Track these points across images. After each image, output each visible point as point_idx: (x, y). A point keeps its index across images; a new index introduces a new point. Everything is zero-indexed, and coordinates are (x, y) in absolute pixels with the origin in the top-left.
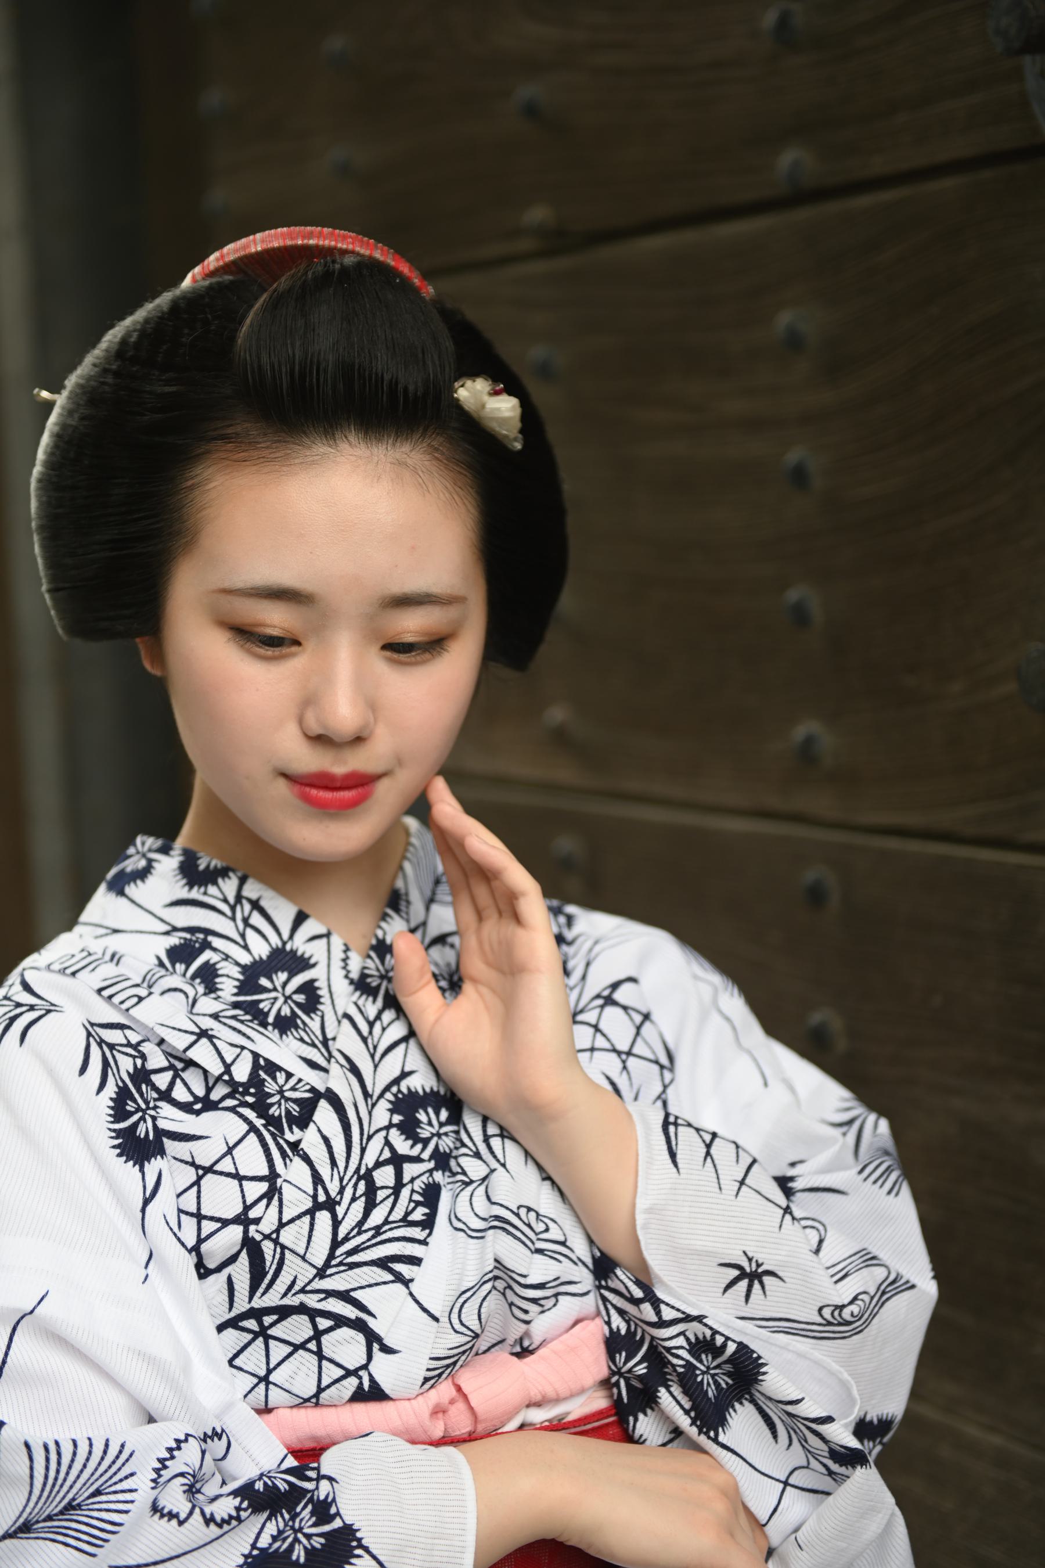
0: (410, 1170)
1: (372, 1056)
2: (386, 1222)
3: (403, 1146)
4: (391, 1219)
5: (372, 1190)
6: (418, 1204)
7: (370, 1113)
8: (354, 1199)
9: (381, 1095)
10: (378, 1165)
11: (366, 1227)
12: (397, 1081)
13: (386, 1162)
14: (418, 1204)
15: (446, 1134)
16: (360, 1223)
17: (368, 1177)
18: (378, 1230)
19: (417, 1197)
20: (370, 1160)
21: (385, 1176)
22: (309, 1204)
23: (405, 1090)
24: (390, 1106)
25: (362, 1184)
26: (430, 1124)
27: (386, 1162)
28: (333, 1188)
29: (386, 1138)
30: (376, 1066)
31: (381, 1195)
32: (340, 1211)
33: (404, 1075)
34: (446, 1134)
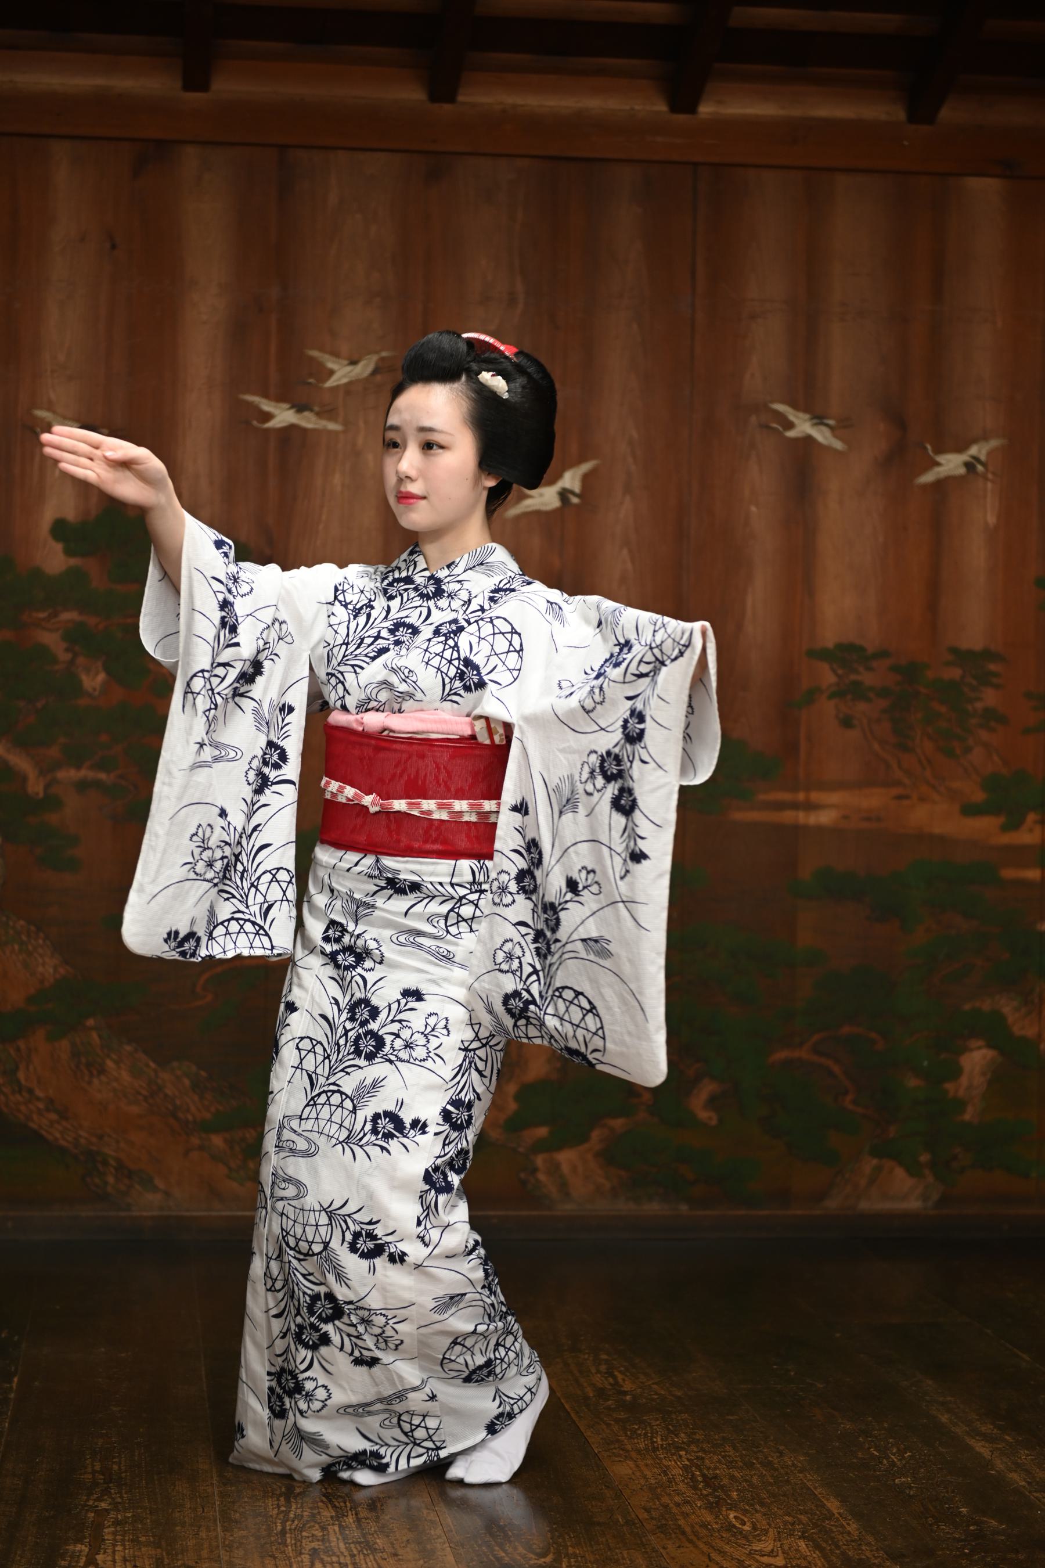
2: (343, 1056)
8: (334, 1052)
22: (322, 1058)
32: (331, 1058)
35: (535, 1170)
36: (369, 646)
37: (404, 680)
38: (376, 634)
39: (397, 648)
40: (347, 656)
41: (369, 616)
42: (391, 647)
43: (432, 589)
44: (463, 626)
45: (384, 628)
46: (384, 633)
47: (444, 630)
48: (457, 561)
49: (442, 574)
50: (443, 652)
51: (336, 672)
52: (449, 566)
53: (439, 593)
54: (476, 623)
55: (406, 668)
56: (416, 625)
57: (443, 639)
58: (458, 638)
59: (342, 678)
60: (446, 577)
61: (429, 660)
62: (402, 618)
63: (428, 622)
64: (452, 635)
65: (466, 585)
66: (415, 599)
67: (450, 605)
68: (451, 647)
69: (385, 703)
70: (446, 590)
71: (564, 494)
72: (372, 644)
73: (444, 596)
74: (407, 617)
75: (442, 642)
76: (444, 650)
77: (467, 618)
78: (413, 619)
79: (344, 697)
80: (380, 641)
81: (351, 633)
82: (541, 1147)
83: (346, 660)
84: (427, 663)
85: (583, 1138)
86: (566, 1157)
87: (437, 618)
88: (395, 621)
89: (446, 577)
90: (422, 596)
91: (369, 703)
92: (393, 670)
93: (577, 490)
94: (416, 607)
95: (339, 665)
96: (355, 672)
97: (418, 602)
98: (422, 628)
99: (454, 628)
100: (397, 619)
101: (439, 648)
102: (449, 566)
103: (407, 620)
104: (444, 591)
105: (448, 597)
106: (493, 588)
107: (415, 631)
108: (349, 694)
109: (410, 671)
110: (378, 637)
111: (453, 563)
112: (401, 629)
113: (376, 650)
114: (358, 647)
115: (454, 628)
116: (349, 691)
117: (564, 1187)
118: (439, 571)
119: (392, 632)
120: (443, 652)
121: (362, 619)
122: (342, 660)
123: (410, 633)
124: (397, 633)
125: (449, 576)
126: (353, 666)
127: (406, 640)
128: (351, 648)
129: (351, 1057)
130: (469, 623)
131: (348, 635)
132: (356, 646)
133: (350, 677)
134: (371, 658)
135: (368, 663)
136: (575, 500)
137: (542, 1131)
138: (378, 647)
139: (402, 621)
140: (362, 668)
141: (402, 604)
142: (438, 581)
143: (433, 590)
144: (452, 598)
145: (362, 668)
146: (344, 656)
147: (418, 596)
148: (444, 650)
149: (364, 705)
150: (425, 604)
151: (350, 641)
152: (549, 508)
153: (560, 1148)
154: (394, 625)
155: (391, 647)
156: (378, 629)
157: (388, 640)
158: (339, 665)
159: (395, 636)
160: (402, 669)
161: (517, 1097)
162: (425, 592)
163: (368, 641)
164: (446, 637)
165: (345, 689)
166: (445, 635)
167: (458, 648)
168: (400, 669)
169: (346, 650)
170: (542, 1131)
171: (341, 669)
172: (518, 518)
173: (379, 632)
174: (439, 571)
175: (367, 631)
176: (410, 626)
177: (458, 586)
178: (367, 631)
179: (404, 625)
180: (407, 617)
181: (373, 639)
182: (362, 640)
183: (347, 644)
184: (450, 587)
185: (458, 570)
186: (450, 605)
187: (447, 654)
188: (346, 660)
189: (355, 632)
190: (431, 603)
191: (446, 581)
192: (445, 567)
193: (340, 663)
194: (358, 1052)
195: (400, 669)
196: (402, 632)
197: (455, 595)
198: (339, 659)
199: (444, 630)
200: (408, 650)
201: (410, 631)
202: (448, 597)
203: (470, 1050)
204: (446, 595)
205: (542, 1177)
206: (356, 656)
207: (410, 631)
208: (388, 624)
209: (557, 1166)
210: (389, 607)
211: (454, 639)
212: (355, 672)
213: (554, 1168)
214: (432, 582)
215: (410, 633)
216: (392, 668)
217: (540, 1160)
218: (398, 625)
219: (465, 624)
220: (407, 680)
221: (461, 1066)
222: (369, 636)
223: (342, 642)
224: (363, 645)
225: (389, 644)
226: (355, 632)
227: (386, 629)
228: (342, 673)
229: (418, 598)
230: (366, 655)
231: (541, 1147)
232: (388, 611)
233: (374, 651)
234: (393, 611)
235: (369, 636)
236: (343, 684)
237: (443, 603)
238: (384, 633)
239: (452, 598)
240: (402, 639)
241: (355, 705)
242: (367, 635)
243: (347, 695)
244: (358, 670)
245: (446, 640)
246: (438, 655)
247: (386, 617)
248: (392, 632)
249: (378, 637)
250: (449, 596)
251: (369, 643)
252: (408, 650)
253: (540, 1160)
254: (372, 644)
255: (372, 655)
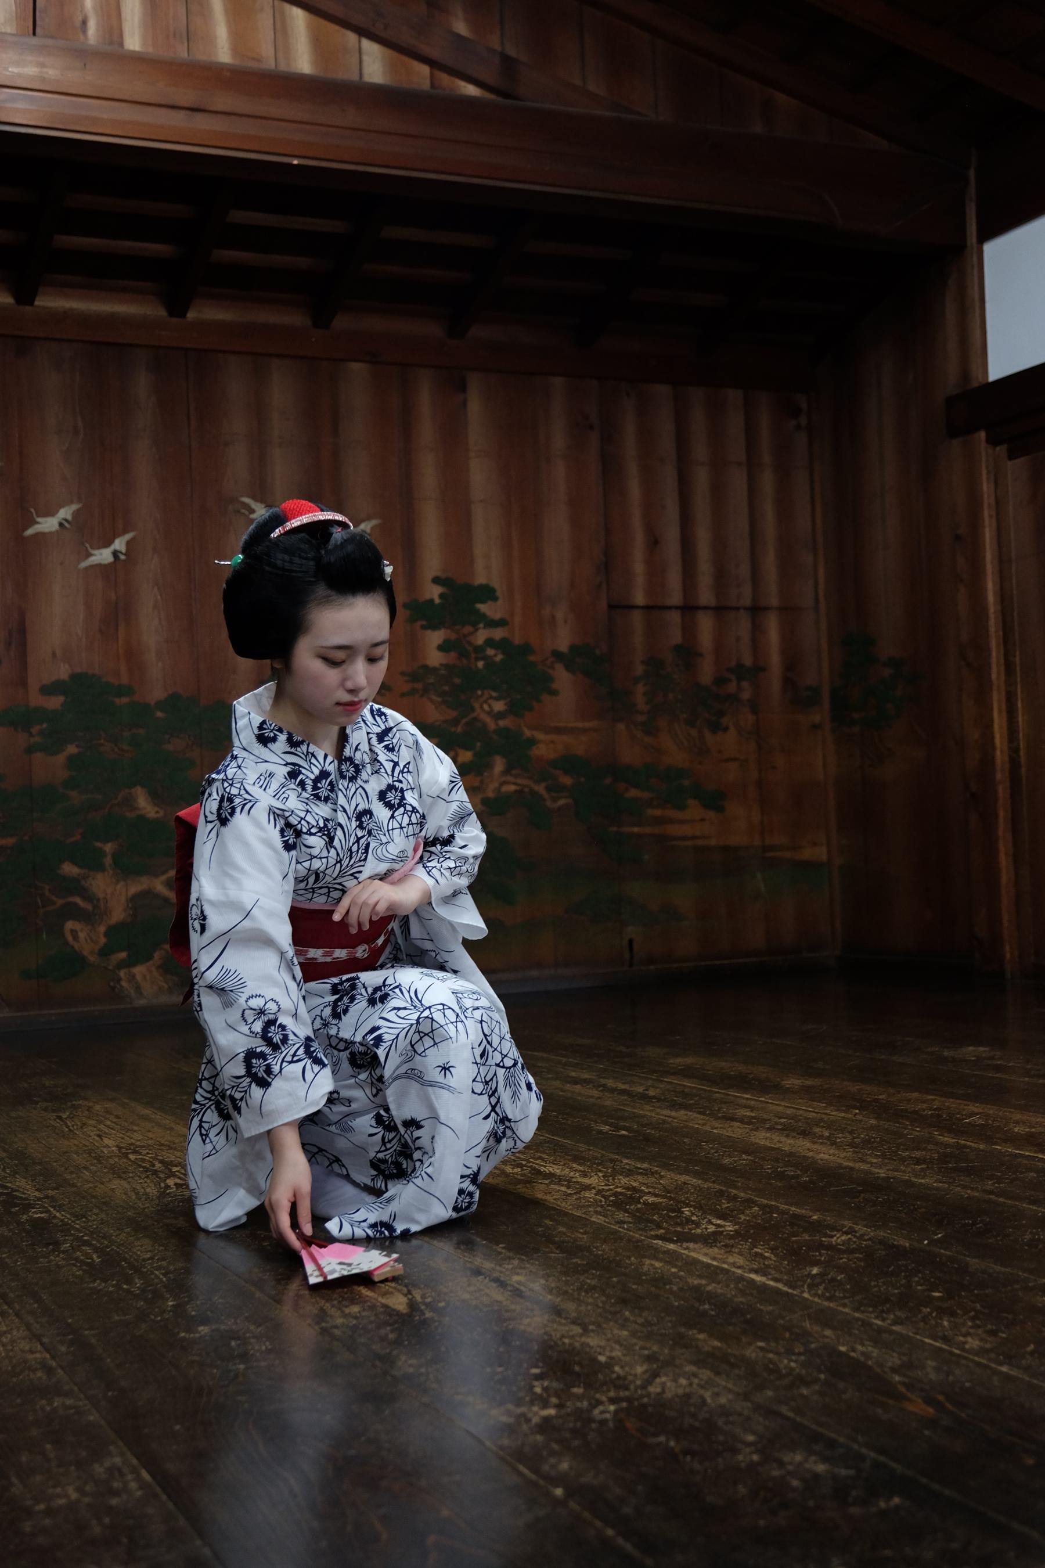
35: (119, 980)
71: (115, 554)
82: (122, 965)
85: (149, 958)
86: (139, 970)
93: (124, 551)
117: (138, 988)
136: (123, 557)
137: (123, 955)
152: (106, 562)
153: (134, 965)
161: (106, 934)
170: (123, 955)
172: (87, 569)
205: (124, 984)
209: (134, 976)
213: (132, 978)
217: (122, 973)
231: (122, 965)
253: (122, 973)
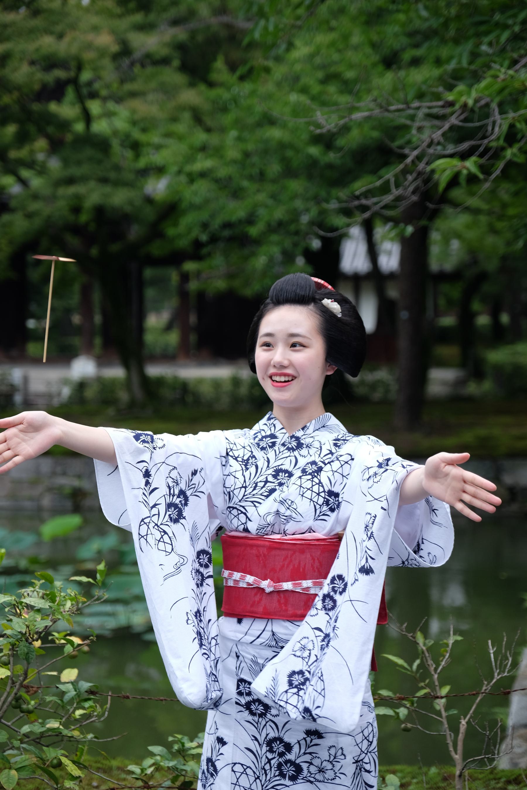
0: (273, 762)
1: (259, 732)
2: (271, 778)
3: (270, 756)
4: (272, 776)
5: (265, 771)
6: (276, 770)
7: (261, 750)
8: (263, 775)
9: (264, 743)
10: (265, 764)
11: (267, 780)
12: (266, 738)
13: (267, 763)
14: (276, 770)
15: (280, 747)
16: (266, 780)
17: (264, 769)
18: (269, 780)
19: (276, 769)
20: (263, 764)
21: (267, 767)
23: (268, 740)
24: (266, 745)
25: (263, 770)
26: (276, 746)
27: (267, 763)
28: (258, 774)
29: (266, 756)
30: (260, 735)
31: (268, 772)
33: (267, 735)
34: (280, 747)
36: (262, 488)
37: (288, 508)
38: (265, 480)
39: (281, 488)
40: (246, 495)
41: (257, 467)
42: (277, 487)
43: (294, 444)
44: (321, 466)
45: (269, 475)
46: (270, 479)
47: (309, 470)
48: (308, 425)
49: (299, 434)
50: (312, 487)
51: (238, 507)
52: (303, 429)
53: (300, 446)
54: (329, 464)
55: (290, 500)
56: (290, 470)
57: (310, 477)
58: (320, 476)
59: (244, 511)
60: (302, 436)
61: (303, 494)
62: (279, 466)
63: (297, 467)
64: (316, 474)
65: (316, 438)
66: (284, 452)
67: (309, 453)
68: (317, 484)
69: (274, 525)
70: (304, 443)
72: (264, 486)
73: (304, 447)
74: (282, 465)
75: (310, 480)
76: (313, 486)
77: (322, 460)
78: (287, 466)
79: (246, 523)
80: (268, 484)
81: (247, 480)
83: (246, 498)
84: (302, 496)
87: (302, 462)
88: (275, 468)
89: (302, 436)
90: (289, 449)
91: (268, 527)
92: (281, 502)
94: (287, 457)
95: (240, 501)
96: (255, 506)
97: (287, 453)
98: (294, 472)
99: (316, 469)
100: (275, 467)
101: (309, 484)
102: (303, 429)
103: (283, 467)
104: (303, 444)
105: (306, 447)
106: (335, 438)
107: (291, 475)
108: (250, 521)
109: (292, 502)
110: (266, 482)
111: (305, 426)
112: (281, 474)
113: (268, 491)
114: (254, 489)
115: (316, 469)
116: (251, 519)
118: (297, 432)
119: (275, 476)
120: (312, 487)
121: (253, 469)
122: (243, 498)
123: (287, 477)
124: (278, 478)
125: (304, 435)
126: (252, 502)
127: (285, 482)
128: (249, 490)
129: (278, 778)
130: (325, 464)
131: (245, 481)
132: (252, 489)
133: (251, 511)
134: (265, 496)
135: (264, 500)
138: (268, 488)
139: (280, 468)
140: (260, 503)
141: (276, 455)
142: (298, 439)
143: (296, 444)
144: (309, 448)
145: (260, 503)
146: (244, 496)
147: (286, 449)
148: (313, 486)
149: (264, 528)
150: (292, 454)
151: (247, 485)
154: (275, 471)
155: (277, 487)
156: (265, 476)
157: (274, 483)
158: (240, 501)
159: (278, 479)
160: (287, 501)
162: (290, 446)
163: (261, 484)
164: (312, 476)
165: (247, 517)
166: (310, 474)
167: (322, 483)
168: (286, 501)
169: (245, 491)
171: (242, 504)
173: (267, 478)
174: (297, 432)
175: (258, 478)
176: (286, 471)
177: (311, 440)
178: (258, 478)
179: (281, 471)
180: (282, 465)
181: (263, 483)
182: (256, 484)
183: (245, 487)
184: (305, 441)
185: (310, 431)
186: (309, 453)
187: (316, 488)
188: (246, 498)
189: (250, 479)
190: (296, 453)
191: (303, 438)
192: (301, 430)
193: (241, 500)
194: (282, 775)
195: (286, 501)
196: (282, 476)
197: (311, 445)
198: (240, 497)
199: (309, 470)
200: (288, 487)
201: (287, 475)
202: (306, 447)
203: (359, 761)
204: (304, 446)
206: (254, 495)
207: (287, 475)
208: (271, 471)
210: (268, 458)
211: (317, 477)
212: (255, 506)
214: (294, 439)
215: (287, 477)
216: (281, 501)
218: (278, 472)
219: (323, 465)
220: (290, 508)
221: (355, 773)
222: (260, 481)
223: (241, 486)
224: (257, 488)
225: (275, 486)
226: (250, 479)
227: (271, 476)
228: (243, 507)
229: (287, 451)
230: (261, 495)
232: (268, 461)
233: (266, 492)
234: (272, 461)
235: (260, 481)
236: (245, 514)
237: (304, 451)
238: (270, 479)
239: (309, 448)
240: (283, 481)
241: (256, 528)
242: (259, 480)
243: (249, 522)
244: (257, 504)
245: (313, 478)
246: (309, 489)
247: (268, 466)
248: (275, 476)
249: (266, 482)
250: (307, 446)
251: (262, 486)
252: (288, 487)
254: (264, 486)
255: (266, 494)
